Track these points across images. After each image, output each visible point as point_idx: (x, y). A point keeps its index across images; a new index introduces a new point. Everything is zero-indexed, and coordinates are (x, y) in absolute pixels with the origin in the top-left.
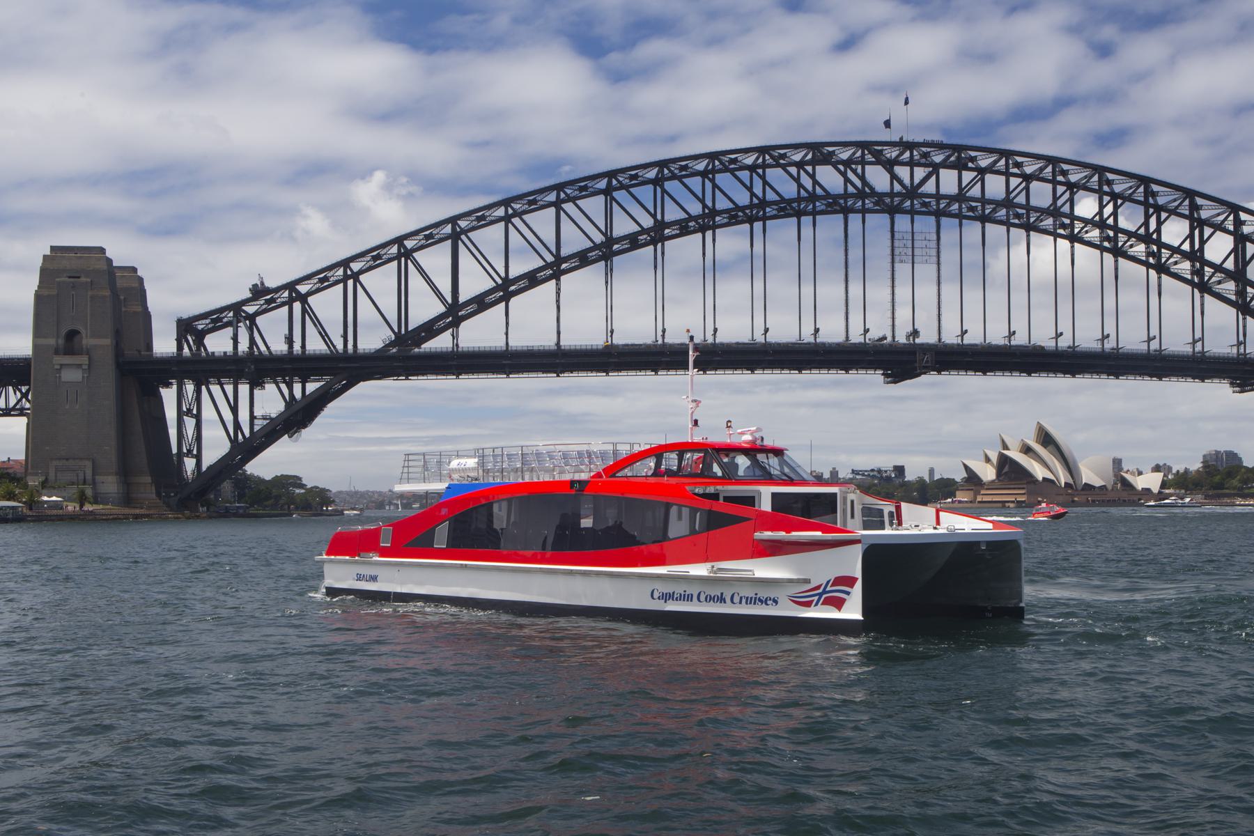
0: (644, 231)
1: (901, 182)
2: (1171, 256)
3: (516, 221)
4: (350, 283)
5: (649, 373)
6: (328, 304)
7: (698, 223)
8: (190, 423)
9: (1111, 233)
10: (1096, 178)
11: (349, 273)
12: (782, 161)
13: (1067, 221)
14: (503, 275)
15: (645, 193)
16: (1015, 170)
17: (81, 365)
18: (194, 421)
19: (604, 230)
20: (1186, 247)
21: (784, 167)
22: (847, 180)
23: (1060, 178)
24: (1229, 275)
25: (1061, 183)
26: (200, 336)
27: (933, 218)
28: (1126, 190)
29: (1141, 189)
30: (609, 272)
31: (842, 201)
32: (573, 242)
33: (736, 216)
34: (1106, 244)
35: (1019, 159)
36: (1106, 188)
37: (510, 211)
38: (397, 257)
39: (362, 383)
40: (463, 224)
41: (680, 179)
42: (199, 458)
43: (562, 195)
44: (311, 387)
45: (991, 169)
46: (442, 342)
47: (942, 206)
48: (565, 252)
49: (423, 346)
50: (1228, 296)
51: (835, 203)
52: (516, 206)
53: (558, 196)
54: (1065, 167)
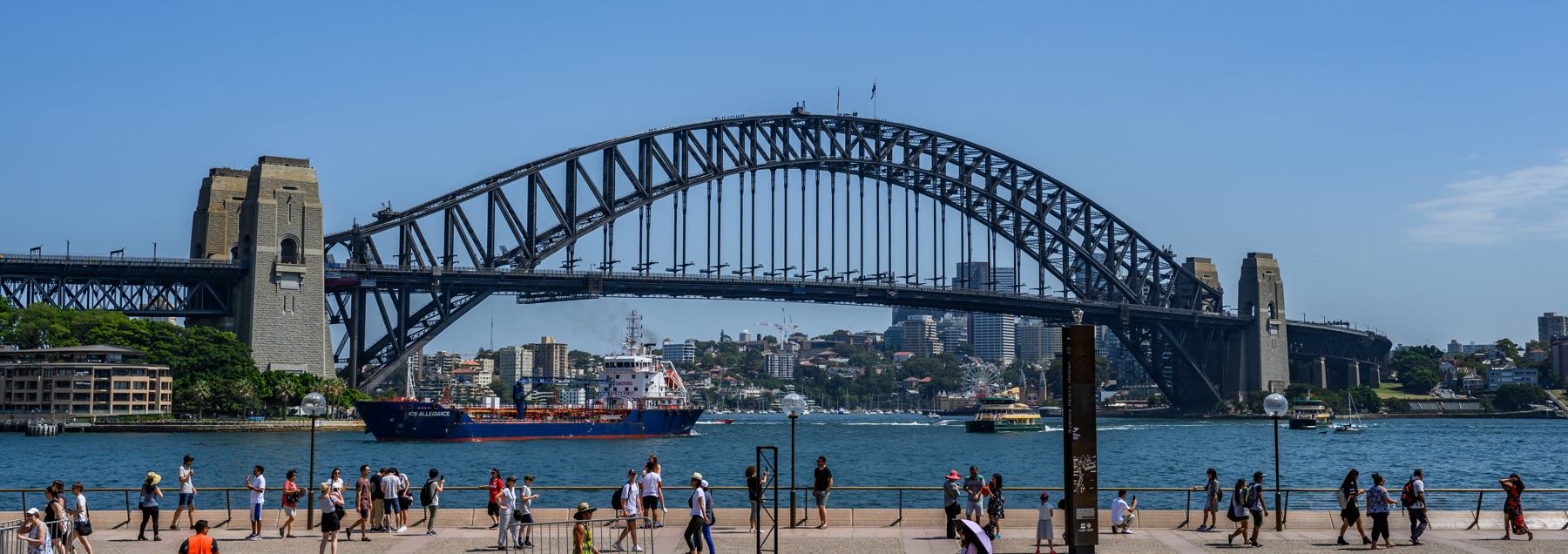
17: (299, 274)
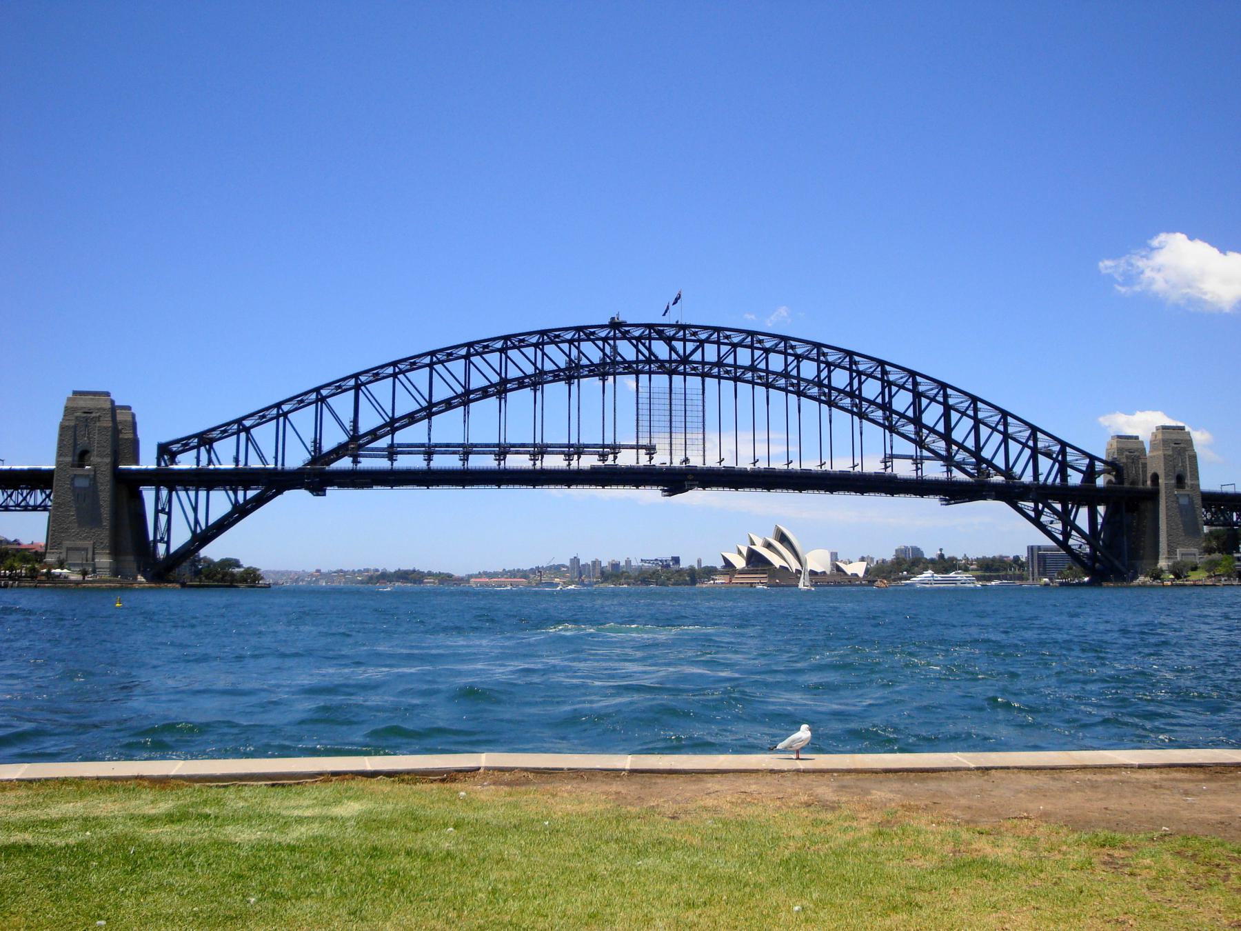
0: (492, 385)
1: (677, 353)
2: (869, 407)
3: (401, 376)
4: (281, 419)
5: (494, 487)
6: (264, 434)
7: (531, 380)
8: (163, 518)
9: (826, 390)
10: (815, 351)
11: (281, 412)
12: (592, 337)
13: (795, 381)
14: (390, 415)
15: (494, 358)
16: (758, 345)
18: (166, 517)
19: (463, 384)
20: (879, 400)
21: (593, 341)
22: (638, 351)
23: (790, 351)
24: (910, 420)
25: (790, 355)
26: (173, 457)
27: (699, 378)
28: (836, 360)
29: (847, 359)
30: (467, 414)
31: (635, 366)
32: (442, 392)
33: (559, 375)
34: (823, 398)
35: (761, 337)
36: (822, 358)
37: (397, 370)
38: (316, 402)
39: (286, 493)
40: (363, 378)
41: (519, 348)
42: (168, 543)
43: (435, 359)
44: (251, 494)
45: (740, 344)
46: (345, 463)
47: (706, 370)
48: (435, 400)
49: (331, 465)
50: (910, 435)
51: (630, 367)
52: (401, 366)
53: (432, 359)
54: (793, 343)
